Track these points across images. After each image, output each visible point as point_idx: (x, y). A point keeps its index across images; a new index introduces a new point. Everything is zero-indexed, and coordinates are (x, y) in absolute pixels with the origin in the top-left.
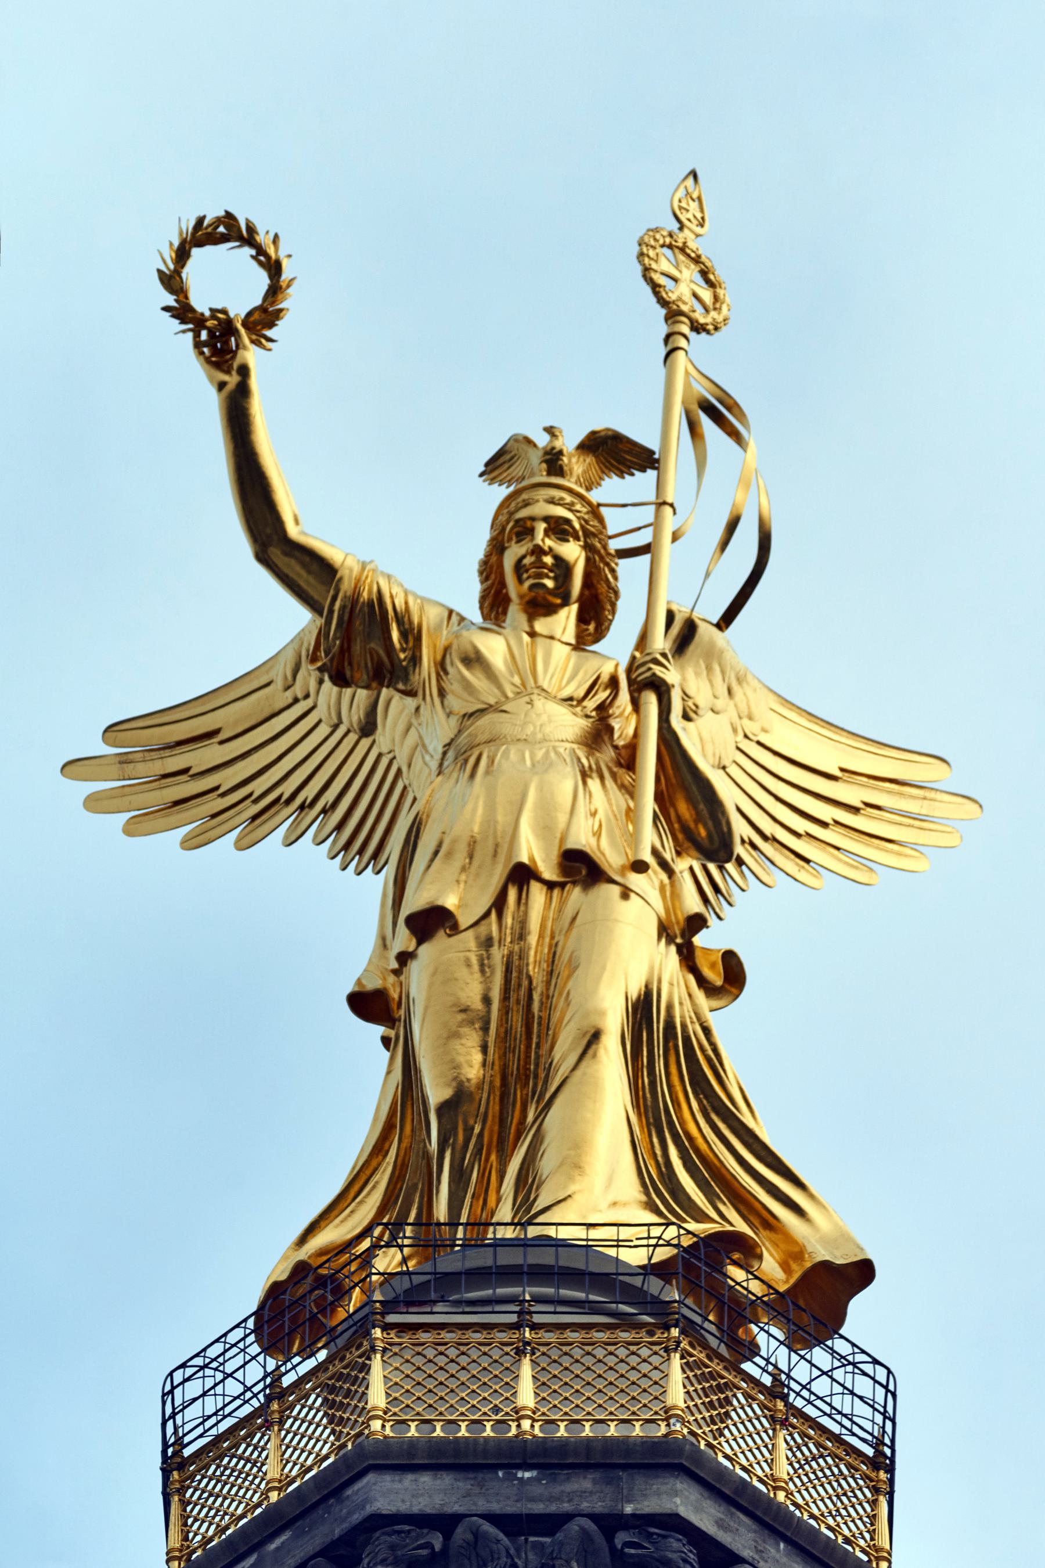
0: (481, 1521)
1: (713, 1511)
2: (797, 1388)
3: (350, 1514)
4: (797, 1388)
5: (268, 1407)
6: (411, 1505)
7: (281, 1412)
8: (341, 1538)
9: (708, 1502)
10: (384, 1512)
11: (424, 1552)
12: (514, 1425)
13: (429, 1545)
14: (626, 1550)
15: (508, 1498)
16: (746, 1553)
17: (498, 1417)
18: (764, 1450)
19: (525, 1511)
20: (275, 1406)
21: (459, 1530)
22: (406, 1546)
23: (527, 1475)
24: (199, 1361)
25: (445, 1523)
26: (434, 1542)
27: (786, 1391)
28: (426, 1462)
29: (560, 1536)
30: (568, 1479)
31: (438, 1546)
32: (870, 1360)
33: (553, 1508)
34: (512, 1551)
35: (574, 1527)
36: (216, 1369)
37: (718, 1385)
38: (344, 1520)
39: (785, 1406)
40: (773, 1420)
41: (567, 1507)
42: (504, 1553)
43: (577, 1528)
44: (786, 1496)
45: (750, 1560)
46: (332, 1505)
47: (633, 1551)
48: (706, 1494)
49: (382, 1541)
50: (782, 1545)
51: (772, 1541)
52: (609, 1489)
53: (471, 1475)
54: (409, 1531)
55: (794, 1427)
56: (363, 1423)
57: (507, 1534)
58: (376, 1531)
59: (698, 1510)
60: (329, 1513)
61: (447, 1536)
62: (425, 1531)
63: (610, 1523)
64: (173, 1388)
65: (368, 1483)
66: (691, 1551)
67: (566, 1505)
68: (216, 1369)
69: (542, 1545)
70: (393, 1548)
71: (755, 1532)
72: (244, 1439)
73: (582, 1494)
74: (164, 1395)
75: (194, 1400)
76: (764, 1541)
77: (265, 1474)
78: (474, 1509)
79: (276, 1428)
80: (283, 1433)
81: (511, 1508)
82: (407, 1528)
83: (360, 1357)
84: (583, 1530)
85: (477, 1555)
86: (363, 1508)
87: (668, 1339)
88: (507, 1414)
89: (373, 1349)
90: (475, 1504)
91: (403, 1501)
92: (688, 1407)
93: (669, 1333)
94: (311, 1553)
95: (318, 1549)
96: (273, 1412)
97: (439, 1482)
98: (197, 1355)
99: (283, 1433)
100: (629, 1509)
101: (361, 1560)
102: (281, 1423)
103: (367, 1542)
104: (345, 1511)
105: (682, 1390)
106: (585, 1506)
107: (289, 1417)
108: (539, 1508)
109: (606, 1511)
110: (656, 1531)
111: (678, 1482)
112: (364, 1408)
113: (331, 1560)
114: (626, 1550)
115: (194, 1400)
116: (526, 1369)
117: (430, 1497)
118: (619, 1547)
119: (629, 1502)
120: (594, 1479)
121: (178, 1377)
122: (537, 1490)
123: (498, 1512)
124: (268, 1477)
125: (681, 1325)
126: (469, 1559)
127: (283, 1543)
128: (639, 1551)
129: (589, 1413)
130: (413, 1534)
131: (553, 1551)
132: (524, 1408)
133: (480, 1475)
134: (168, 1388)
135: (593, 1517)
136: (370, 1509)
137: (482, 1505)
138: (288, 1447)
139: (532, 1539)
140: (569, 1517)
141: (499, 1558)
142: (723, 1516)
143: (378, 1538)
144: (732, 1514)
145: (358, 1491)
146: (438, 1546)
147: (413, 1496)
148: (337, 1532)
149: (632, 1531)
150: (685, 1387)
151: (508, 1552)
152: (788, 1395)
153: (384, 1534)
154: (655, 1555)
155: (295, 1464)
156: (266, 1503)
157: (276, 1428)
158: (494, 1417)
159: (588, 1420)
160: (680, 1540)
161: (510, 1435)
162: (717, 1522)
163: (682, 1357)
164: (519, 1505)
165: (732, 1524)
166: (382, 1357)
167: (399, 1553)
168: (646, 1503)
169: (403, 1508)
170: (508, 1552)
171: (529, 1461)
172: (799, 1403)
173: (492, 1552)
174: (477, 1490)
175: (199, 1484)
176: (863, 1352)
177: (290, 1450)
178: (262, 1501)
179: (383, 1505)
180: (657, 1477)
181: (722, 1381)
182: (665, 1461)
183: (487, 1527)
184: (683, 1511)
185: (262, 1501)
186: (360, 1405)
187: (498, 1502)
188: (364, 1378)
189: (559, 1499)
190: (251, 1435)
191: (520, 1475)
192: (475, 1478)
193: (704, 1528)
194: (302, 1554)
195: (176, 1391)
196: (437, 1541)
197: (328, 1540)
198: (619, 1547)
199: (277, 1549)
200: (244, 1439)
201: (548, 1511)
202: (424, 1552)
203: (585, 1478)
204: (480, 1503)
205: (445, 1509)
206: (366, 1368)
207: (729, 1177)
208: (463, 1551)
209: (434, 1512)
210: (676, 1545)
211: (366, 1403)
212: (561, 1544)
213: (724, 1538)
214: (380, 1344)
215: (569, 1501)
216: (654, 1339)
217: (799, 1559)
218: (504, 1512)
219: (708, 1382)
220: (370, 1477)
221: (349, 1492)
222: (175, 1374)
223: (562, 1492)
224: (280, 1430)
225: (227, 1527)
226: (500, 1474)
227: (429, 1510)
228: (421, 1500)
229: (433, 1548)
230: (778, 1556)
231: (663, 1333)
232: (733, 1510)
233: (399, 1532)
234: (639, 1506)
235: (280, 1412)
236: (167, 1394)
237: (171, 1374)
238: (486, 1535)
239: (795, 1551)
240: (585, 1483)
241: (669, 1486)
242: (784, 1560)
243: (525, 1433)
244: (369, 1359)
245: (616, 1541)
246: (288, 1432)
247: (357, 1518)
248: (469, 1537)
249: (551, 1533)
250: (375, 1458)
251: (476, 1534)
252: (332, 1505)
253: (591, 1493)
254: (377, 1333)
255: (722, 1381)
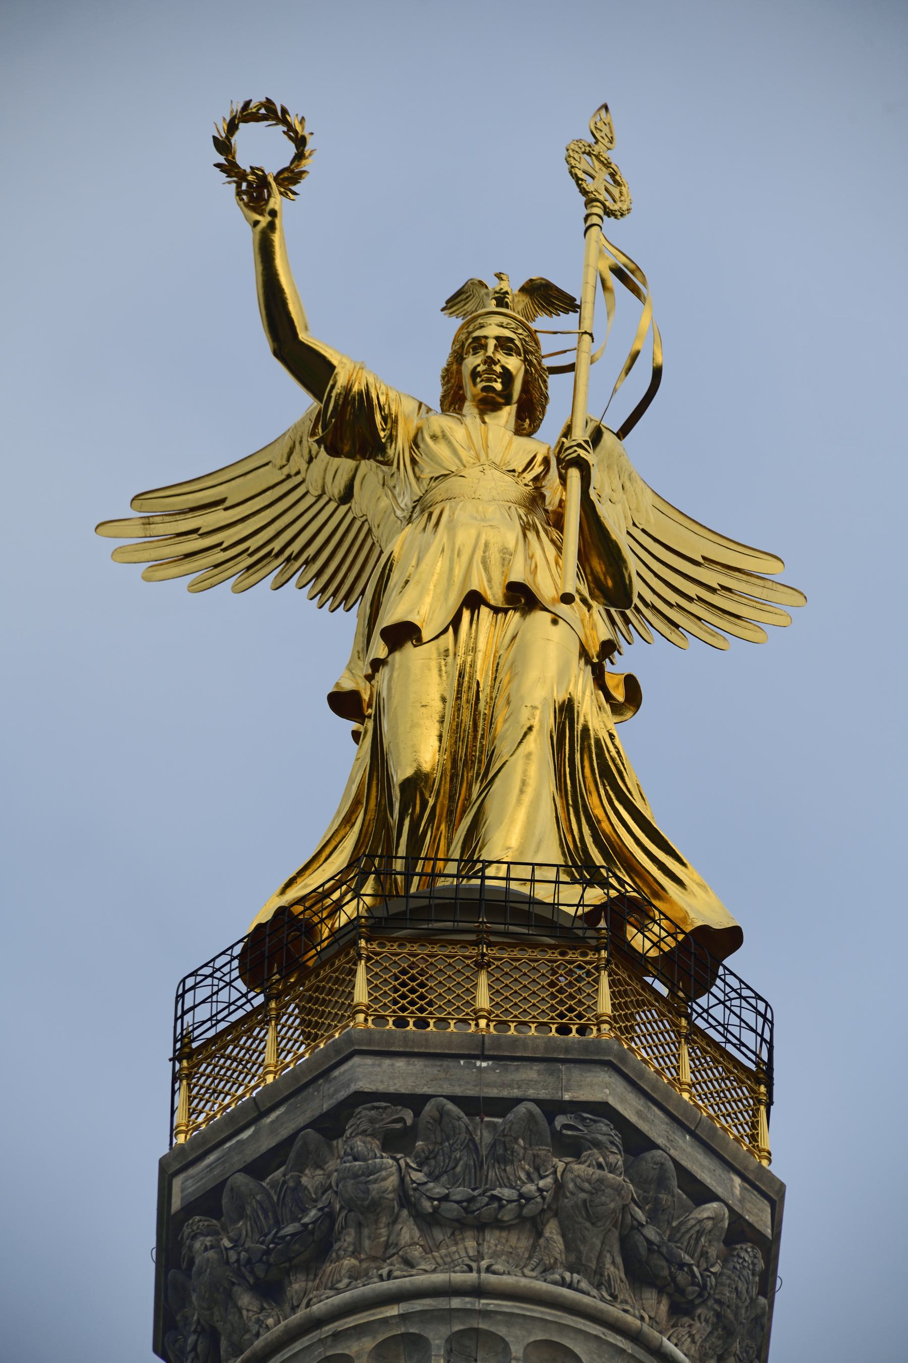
0: (445, 1101)
1: (635, 1103)
2: (700, 1011)
3: (336, 1091)
4: (700, 1011)
5: (268, 1005)
6: (388, 1086)
7: (278, 1009)
8: (328, 1112)
9: (631, 1095)
10: (366, 1090)
11: (398, 1126)
12: (473, 1023)
13: (402, 1120)
14: (564, 1131)
15: (468, 1083)
16: (660, 1141)
17: (460, 1017)
18: (672, 1058)
19: (483, 1095)
20: (273, 1005)
21: (428, 1107)
22: (382, 1120)
23: (484, 1064)
24: (207, 971)
25: (416, 1101)
26: (406, 1117)
27: (689, 1011)
28: (401, 1049)
29: (510, 1116)
30: (517, 1069)
31: (409, 1122)
32: (753, 995)
33: (505, 1093)
34: (470, 1128)
35: (522, 1109)
36: (220, 979)
37: (637, 1000)
38: (331, 1096)
39: (688, 1024)
40: (678, 1034)
41: (516, 1093)
42: (464, 1129)
43: (524, 1110)
44: (690, 1098)
45: (663, 1147)
46: (320, 1085)
47: (569, 1133)
48: (629, 1088)
49: (364, 1113)
50: (688, 1137)
51: (680, 1133)
52: (551, 1080)
53: (439, 1063)
54: (385, 1108)
55: (695, 1042)
56: (349, 1017)
57: (467, 1115)
58: (357, 1107)
59: (622, 1100)
60: (318, 1091)
61: (417, 1114)
62: (399, 1108)
63: (552, 1108)
64: (185, 992)
65: (352, 1066)
66: (616, 1135)
67: (515, 1091)
68: (220, 979)
69: (495, 1125)
70: (372, 1121)
71: (667, 1124)
72: (245, 1032)
73: (529, 1083)
74: (177, 997)
75: (203, 1002)
76: (674, 1133)
77: (263, 1060)
78: (440, 1091)
79: (273, 1023)
80: (279, 1027)
81: (471, 1092)
82: (384, 1104)
83: (347, 963)
84: (530, 1113)
85: (442, 1130)
86: (348, 1086)
87: (599, 959)
88: (467, 1014)
89: (360, 956)
90: (441, 1087)
91: (382, 1082)
92: (614, 1016)
93: (599, 954)
94: (302, 1125)
95: (308, 1121)
96: (271, 1009)
97: (411, 1067)
98: (206, 965)
99: (279, 1027)
100: (567, 1097)
101: (344, 1131)
102: (278, 1018)
103: (350, 1116)
104: (332, 1089)
105: (610, 1002)
106: (531, 1093)
107: (284, 1014)
108: (494, 1092)
109: (548, 1097)
110: (589, 1116)
111: (607, 1076)
112: (350, 1005)
113: (318, 1130)
114: (564, 1131)
115: (203, 1002)
116: (483, 980)
117: (404, 1079)
118: (559, 1128)
119: (567, 1090)
120: (538, 1071)
121: (190, 982)
122: (492, 1077)
123: (460, 1094)
124: (266, 1063)
125: (609, 948)
126: (434, 1134)
127: (277, 1117)
128: (575, 1133)
129: (534, 1017)
130: (389, 1110)
131: (504, 1129)
132: (482, 1010)
133: (445, 1063)
134: (180, 992)
135: (538, 1102)
136: (353, 1088)
137: (447, 1089)
138: (283, 1038)
139: (486, 1119)
140: (518, 1101)
141: (459, 1134)
142: (639, 1107)
143: (359, 1113)
144: (649, 1108)
145: (344, 1072)
146: (409, 1122)
147: (390, 1078)
148: (326, 1107)
149: (569, 1115)
150: (612, 1000)
151: (467, 1127)
152: (692, 1014)
153: (365, 1109)
154: (588, 1137)
155: (289, 1052)
156: (263, 1085)
157: (273, 1023)
158: (457, 1017)
159: (533, 1023)
160: (608, 1125)
161: (470, 1031)
162: (637, 1113)
163: (609, 975)
164: (477, 1089)
165: (649, 1116)
166: (366, 963)
167: (377, 1126)
168: (582, 1092)
169: (381, 1088)
170: (467, 1127)
171: (486, 1053)
172: (700, 1023)
173: (454, 1127)
174: (443, 1075)
175: (198, 1081)
176: (748, 987)
177: (284, 1042)
178: (260, 1083)
179: (365, 1085)
180: (590, 1071)
181: (640, 998)
182: (596, 1058)
183: (450, 1106)
184: (611, 1101)
185: (260, 1083)
186: (347, 1002)
187: (460, 1086)
188: (350, 980)
189: (510, 1086)
190: (251, 1029)
191: (478, 1063)
192: (441, 1065)
193: (627, 1117)
194: (294, 1126)
195: (186, 995)
196: (408, 1116)
197: (317, 1114)
198: (559, 1128)
199: (272, 1122)
200: (245, 1032)
201: (501, 1095)
202: (398, 1126)
203: (531, 1069)
204: (445, 1086)
205: (417, 1090)
206: (353, 973)
207: (629, 855)
208: (429, 1126)
209: (407, 1092)
210: (605, 1129)
211: (352, 1001)
212: (512, 1122)
213: (644, 1127)
214: (363, 952)
215: (519, 1088)
216: (588, 959)
217: (700, 1151)
218: (464, 1094)
219: (629, 997)
220: (356, 1060)
221: (336, 1073)
222: (187, 980)
223: (513, 1080)
224: (276, 1025)
225: (228, 1106)
226: (462, 1062)
227: (403, 1091)
228: (396, 1081)
229: (405, 1123)
230: (684, 1146)
231: (594, 955)
232: (650, 1104)
233: (378, 1108)
234: (575, 1095)
235: (276, 1009)
236: (180, 997)
237: (183, 981)
238: (448, 1113)
239: (697, 1143)
240: (531, 1073)
241: (600, 1079)
242: (689, 1150)
243: (482, 1030)
244: (356, 965)
245: (556, 1123)
246: (283, 1026)
247: (342, 1095)
248: (437, 1114)
249: (503, 1116)
250: (359, 1044)
251: (441, 1111)
252: (320, 1085)
253: (536, 1081)
254: (363, 943)
255: (640, 998)
